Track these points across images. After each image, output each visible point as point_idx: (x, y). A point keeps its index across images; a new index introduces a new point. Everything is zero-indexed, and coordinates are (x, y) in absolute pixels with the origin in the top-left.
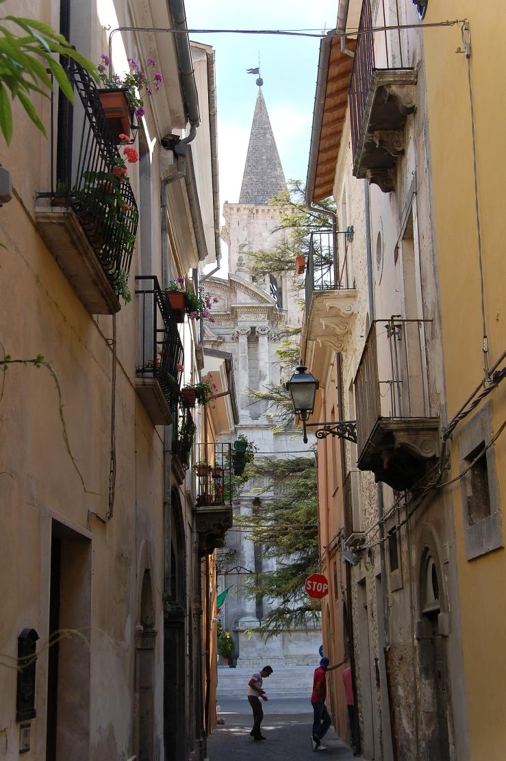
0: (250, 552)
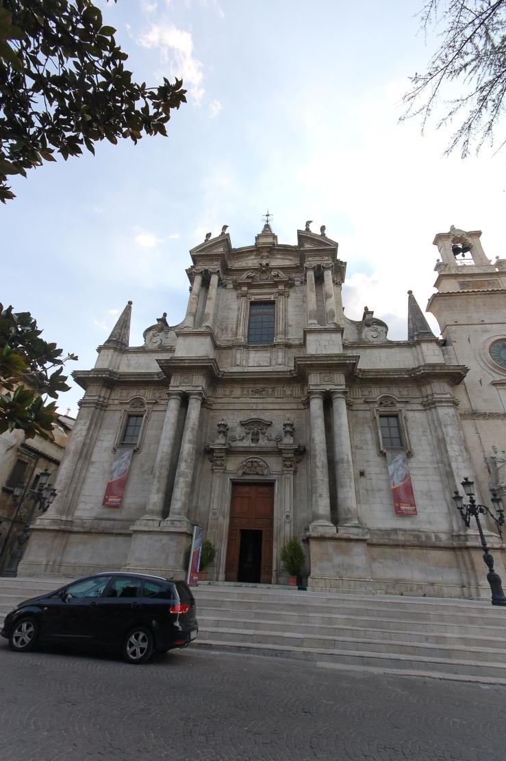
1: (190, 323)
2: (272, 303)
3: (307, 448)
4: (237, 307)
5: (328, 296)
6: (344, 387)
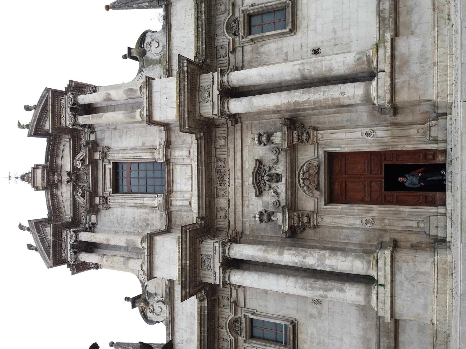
0: (283, 96)
1: (135, 264)
2: (116, 166)
3: (287, 117)
4: (120, 210)
5: (108, 99)
6: (215, 74)
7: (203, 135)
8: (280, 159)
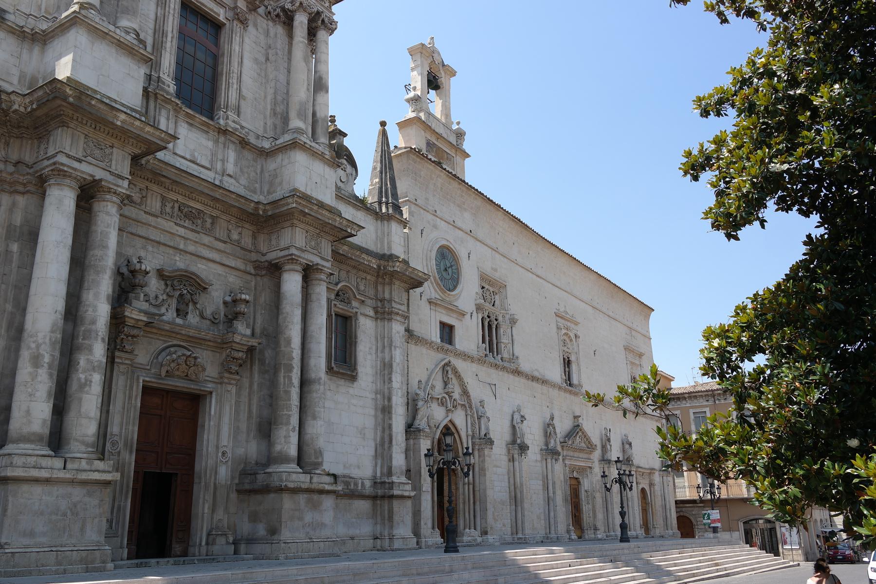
2: (217, 26)
6: (328, 265)
7: (259, 214)
8: (204, 321)
